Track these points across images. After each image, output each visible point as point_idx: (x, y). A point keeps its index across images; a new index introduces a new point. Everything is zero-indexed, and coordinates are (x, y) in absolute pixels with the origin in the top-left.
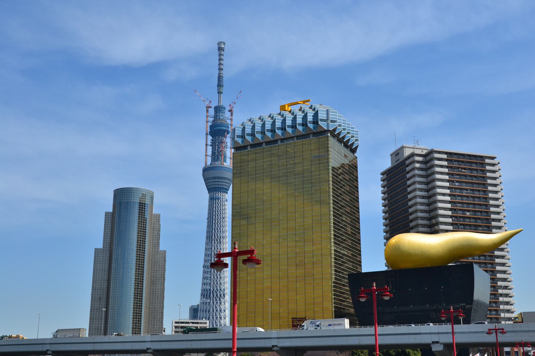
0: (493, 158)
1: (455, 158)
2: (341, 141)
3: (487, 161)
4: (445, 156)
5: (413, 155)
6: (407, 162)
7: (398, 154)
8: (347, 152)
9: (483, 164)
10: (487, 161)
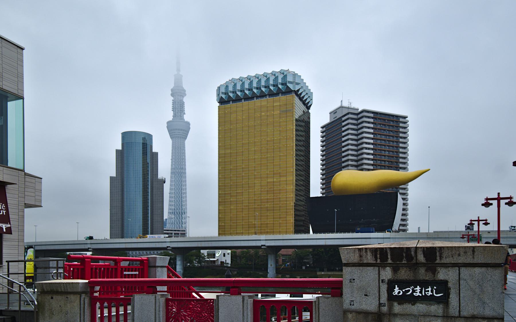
0: (405, 117)
1: (379, 116)
2: (301, 99)
3: (401, 120)
4: (372, 115)
5: (348, 114)
6: (343, 119)
7: (336, 112)
8: (303, 108)
9: (398, 122)
10: (401, 120)
